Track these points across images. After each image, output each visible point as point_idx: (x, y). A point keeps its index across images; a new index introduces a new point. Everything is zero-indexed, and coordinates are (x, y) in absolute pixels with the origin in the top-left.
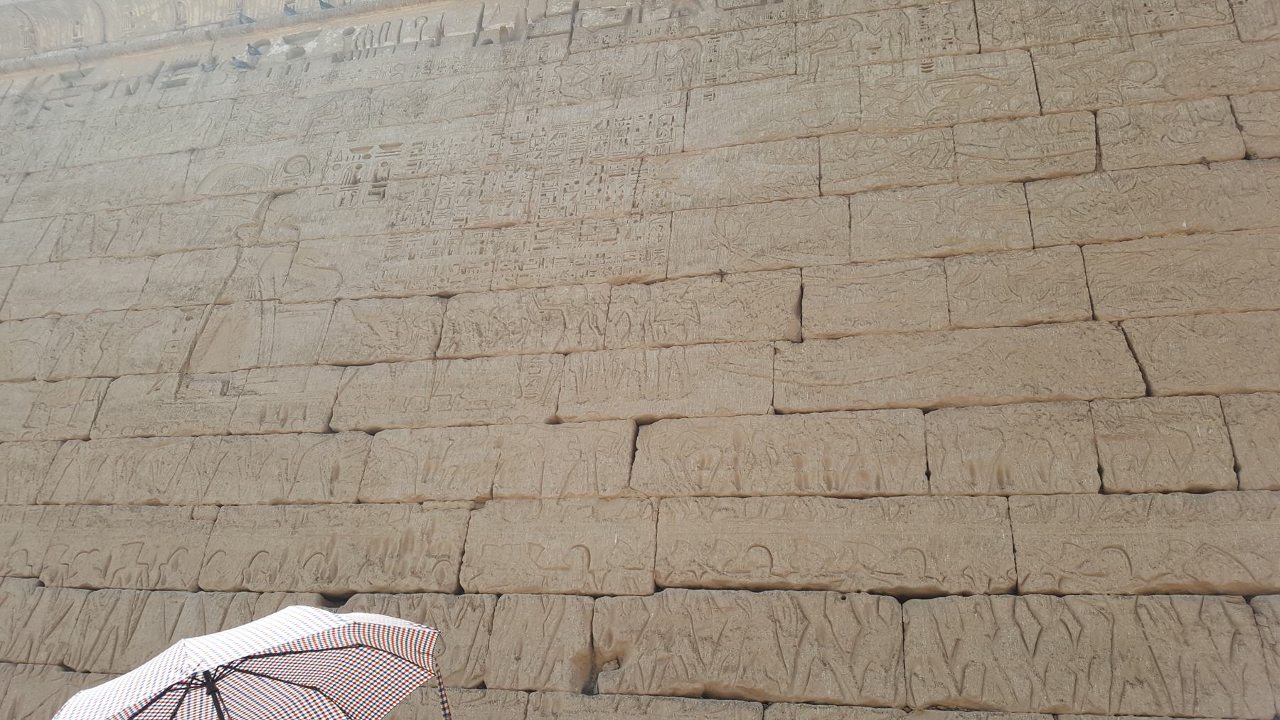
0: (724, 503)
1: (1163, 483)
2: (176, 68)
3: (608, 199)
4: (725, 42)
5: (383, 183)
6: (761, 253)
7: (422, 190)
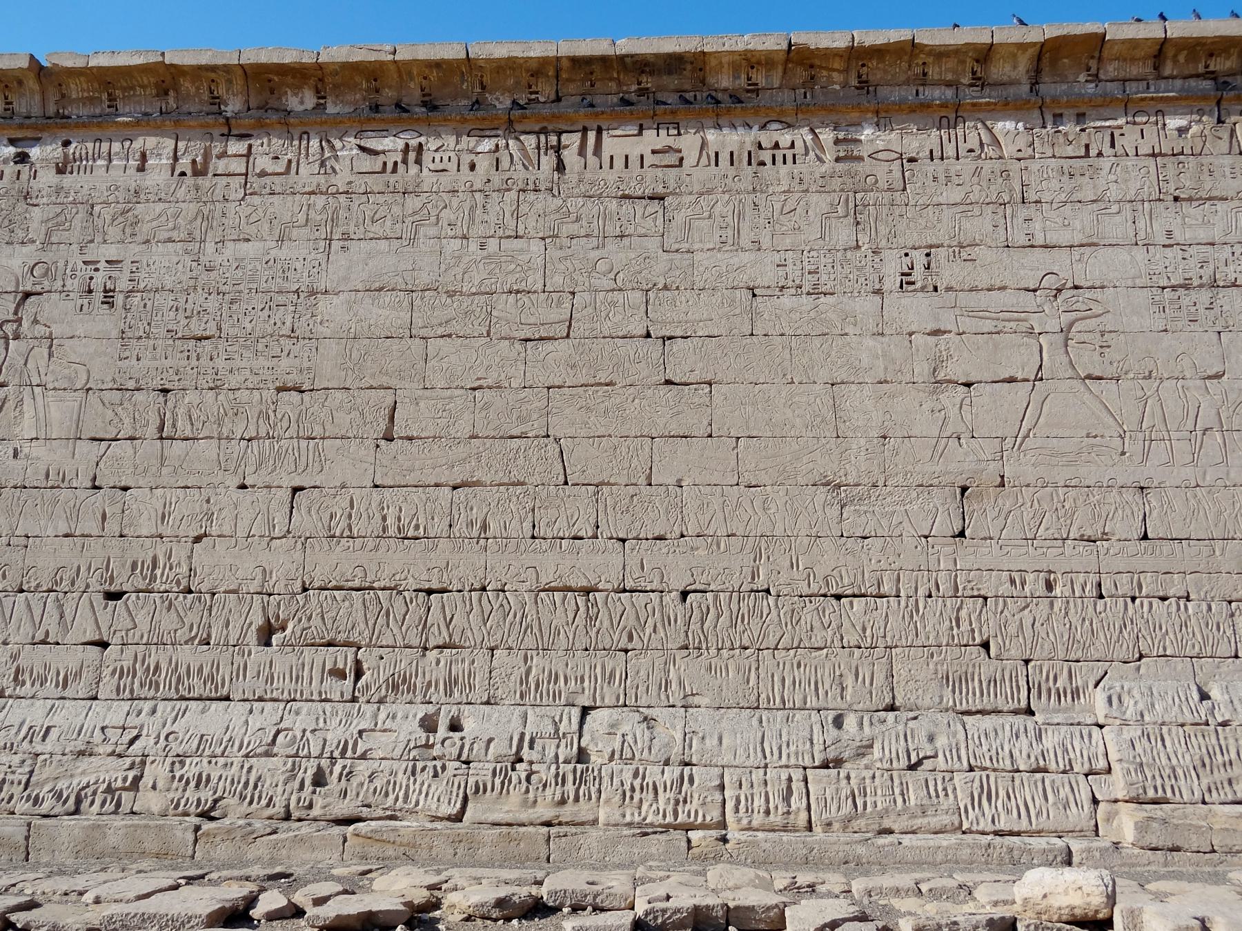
3: (275, 324)
5: (111, 294)
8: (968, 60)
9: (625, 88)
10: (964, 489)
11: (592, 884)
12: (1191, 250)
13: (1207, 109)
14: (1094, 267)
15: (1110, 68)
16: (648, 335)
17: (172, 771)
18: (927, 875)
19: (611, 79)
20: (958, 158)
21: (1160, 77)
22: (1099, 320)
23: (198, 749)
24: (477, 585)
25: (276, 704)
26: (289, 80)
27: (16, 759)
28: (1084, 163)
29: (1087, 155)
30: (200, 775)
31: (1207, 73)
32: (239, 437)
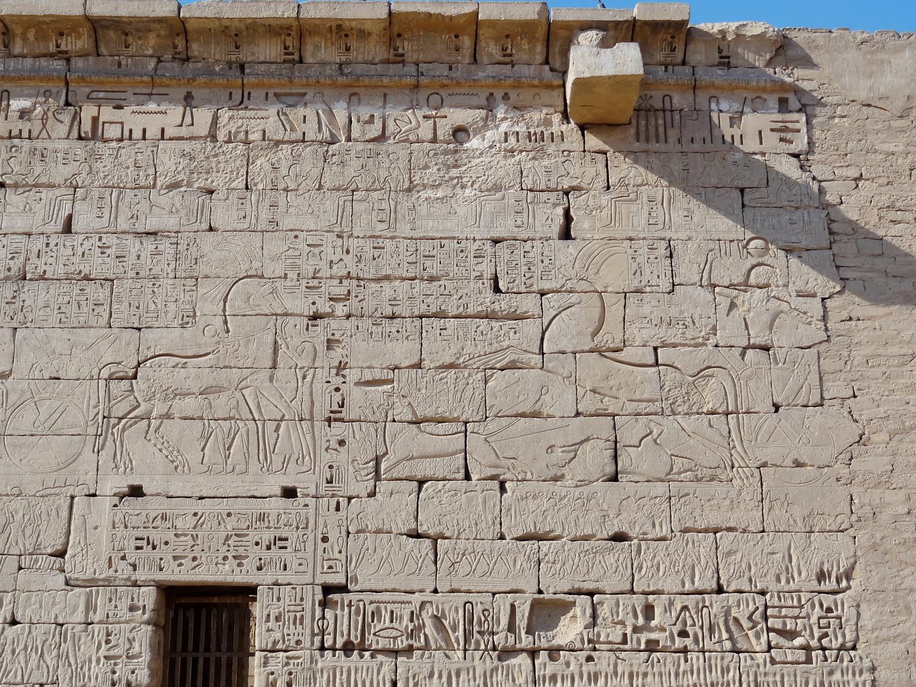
13: (54, 90)
21: (10, 55)
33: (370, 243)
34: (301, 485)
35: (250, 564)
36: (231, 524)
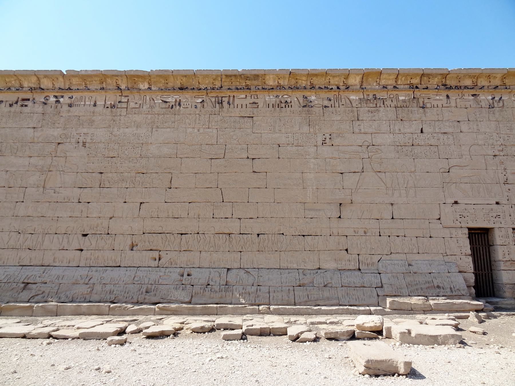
0: (156, 219)
1: (221, 217)
2: (23, 100)
3: (135, 153)
4: (161, 117)
5: (85, 143)
6: (165, 169)
7: (94, 146)
8: (342, 78)
9: (241, 84)
10: (340, 204)
11: (230, 321)
12: (406, 135)
14: (378, 140)
15: (383, 82)
16: (248, 158)
17: (102, 289)
18: (329, 318)
19: (237, 81)
20: (339, 107)
22: (380, 155)
23: (110, 281)
24: (197, 232)
25: (134, 268)
26: (140, 80)
27: (54, 285)
28: (375, 109)
29: (376, 107)
30: (111, 290)
31: (410, 84)
32: (124, 187)
33: (506, 136)
34: (501, 201)
35: (492, 222)
36: (484, 211)
